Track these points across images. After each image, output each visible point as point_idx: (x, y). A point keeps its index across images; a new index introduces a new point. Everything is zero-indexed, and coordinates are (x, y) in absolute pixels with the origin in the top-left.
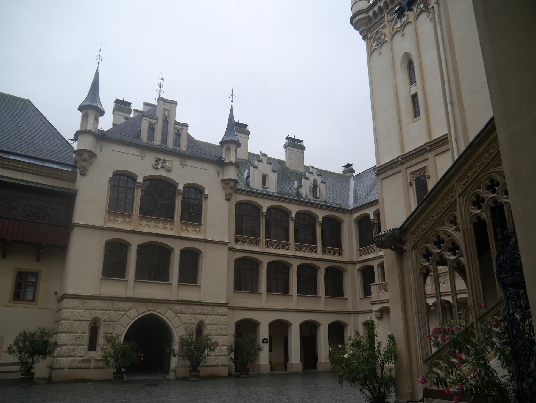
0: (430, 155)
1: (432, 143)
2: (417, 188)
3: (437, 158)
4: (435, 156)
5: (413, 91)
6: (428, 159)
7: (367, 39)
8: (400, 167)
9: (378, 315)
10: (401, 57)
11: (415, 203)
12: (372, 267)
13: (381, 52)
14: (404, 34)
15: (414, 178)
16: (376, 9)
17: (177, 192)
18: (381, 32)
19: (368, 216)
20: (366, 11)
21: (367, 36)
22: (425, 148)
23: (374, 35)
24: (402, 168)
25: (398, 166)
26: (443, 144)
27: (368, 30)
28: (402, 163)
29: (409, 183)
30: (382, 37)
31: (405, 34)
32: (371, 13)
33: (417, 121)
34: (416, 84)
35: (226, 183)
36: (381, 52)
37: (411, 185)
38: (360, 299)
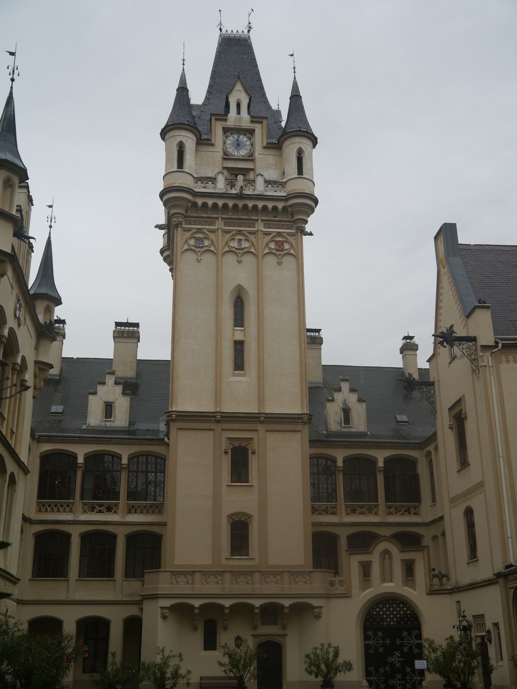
0: (259, 427)
1: (268, 416)
2: (232, 459)
3: (269, 434)
4: (267, 431)
5: (239, 336)
6: (257, 431)
7: (182, 228)
8: (213, 424)
9: (167, 613)
10: (232, 287)
11: (228, 477)
12: (68, 536)
13: (201, 259)
14: (241, 261)
15: (230, 445)
16: (210, 202)
17: (377, 469)
18: (206, 234)
19: (74, 457)
20: (195, 194)
21: (182, 225)
22: (258, 418)
23: (194, 231)
24: (218, 427)
26: (281, 422)
27: (185, 217)
28: (218, 422)
29: (223, 451)
30: (206, 243)
31: (242, 262)
32: (200, 201)
33: (239, 375)
34: (244, 330)
35: (40, 369)
36: (201, 259)
37: (226, 453)
38: (30, 580)
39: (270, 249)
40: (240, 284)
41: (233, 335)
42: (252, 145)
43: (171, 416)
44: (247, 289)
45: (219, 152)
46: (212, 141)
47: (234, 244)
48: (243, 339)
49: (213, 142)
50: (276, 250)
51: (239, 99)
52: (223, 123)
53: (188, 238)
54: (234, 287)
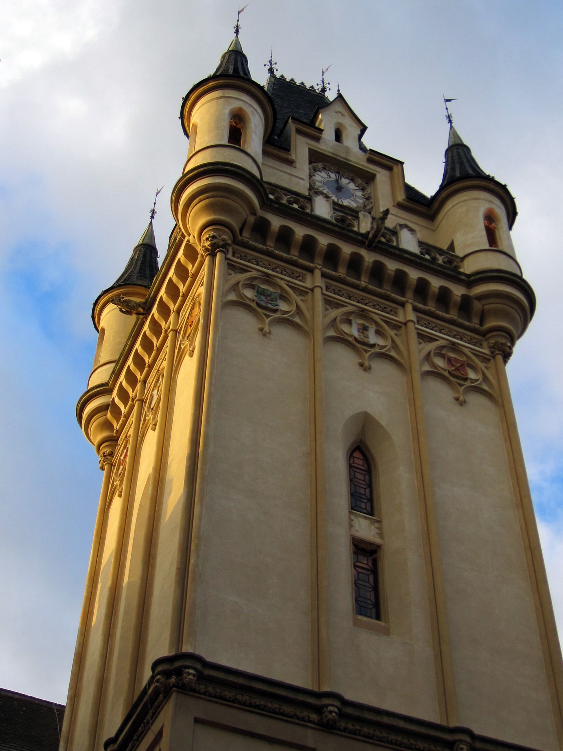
8: (310, 732)
25: (303, 722)
39: (434, 365)
40: (370, 411)
41: (351, 526)
42: (368, 199)
43: (179, 672)
44: (385, 427)
45: (304, 180)
46: (291, 155)
47: (354, 331)
48: (378, 541)
49: (293, 157)
50: (449, 372)
51: (340, 124)
52: (313, 143)
53: (238, 283)
54: (358, 414)
